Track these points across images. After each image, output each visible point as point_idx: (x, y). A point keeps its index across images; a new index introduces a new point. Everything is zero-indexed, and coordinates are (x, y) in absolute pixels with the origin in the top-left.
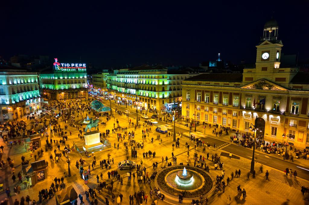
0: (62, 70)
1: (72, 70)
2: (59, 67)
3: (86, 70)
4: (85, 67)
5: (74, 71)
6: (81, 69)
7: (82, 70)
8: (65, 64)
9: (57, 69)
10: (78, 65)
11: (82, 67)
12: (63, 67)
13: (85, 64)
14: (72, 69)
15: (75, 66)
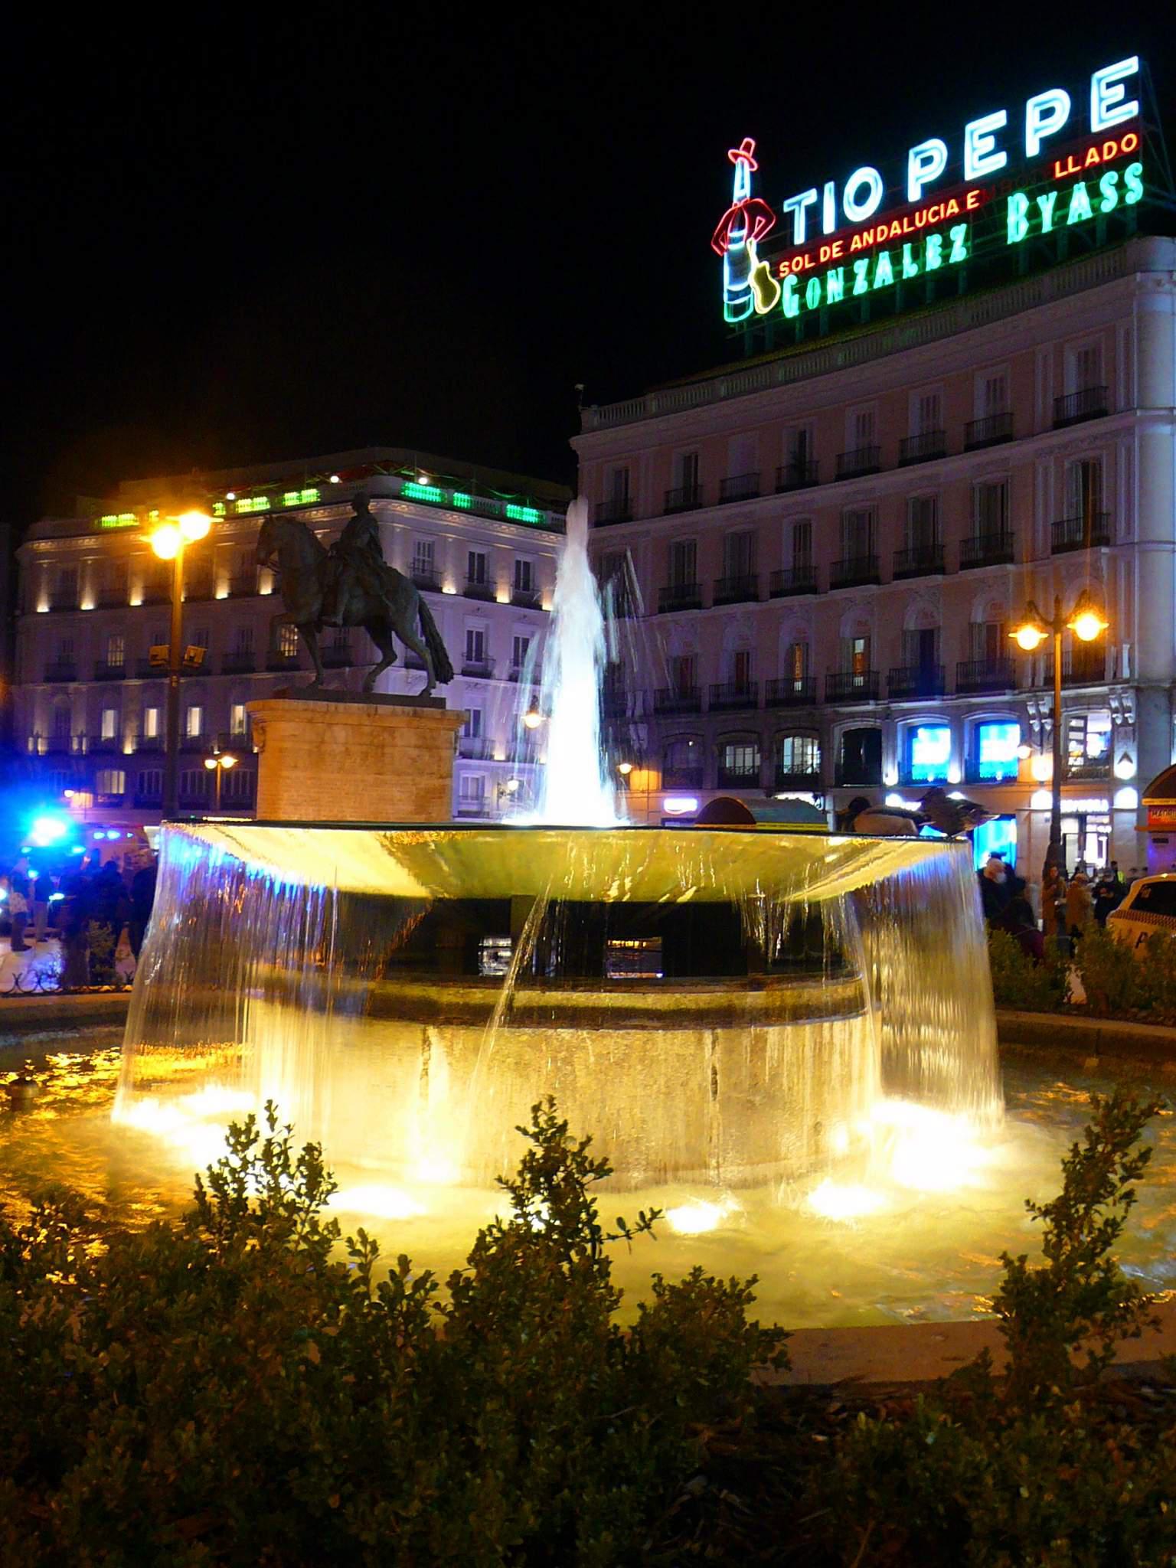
0: (791, 310)
1: (910, 270)
2: (761, 276)
3: (1135, 192)
4: (1115, 133)
5: (948, 270)
6: (1047, 204)
7: (1080, 206)
8: (829, 187)
9: (738, 310)
10: (1010, 139)
11: (1076, 134)
12: (801, 251)
13: (1130, 66)
14: (918, 255)
15: (951, 183)
